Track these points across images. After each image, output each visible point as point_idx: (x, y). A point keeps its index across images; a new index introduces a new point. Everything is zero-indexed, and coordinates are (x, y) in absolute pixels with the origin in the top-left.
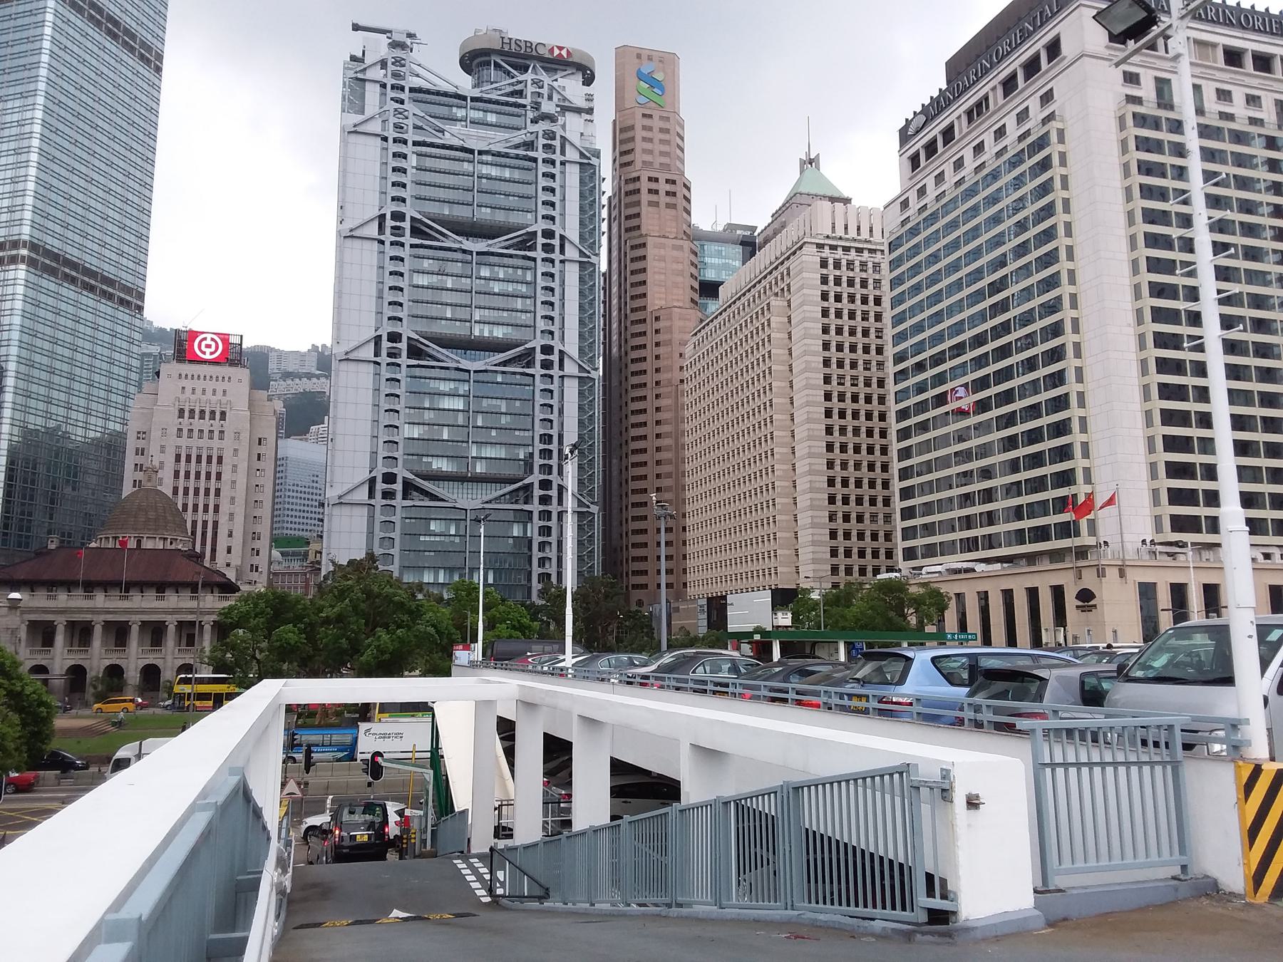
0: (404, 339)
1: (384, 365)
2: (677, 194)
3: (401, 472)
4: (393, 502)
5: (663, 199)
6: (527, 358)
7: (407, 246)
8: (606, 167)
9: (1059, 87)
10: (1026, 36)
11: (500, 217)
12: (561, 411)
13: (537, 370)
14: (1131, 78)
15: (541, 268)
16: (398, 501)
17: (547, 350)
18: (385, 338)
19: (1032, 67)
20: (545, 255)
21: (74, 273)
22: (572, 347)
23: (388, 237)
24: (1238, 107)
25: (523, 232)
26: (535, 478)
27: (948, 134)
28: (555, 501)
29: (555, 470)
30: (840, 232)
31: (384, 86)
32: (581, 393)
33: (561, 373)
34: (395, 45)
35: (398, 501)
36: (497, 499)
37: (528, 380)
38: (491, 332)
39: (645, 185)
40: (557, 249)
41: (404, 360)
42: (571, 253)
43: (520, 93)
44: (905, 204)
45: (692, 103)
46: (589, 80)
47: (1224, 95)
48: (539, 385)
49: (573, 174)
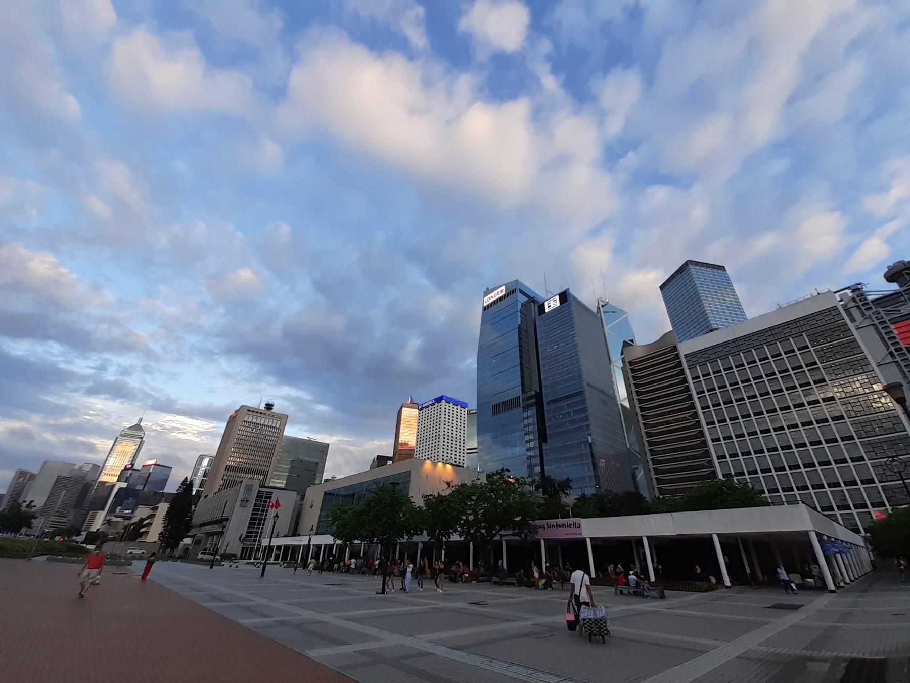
31: (858, 306)
34: (853, 291)
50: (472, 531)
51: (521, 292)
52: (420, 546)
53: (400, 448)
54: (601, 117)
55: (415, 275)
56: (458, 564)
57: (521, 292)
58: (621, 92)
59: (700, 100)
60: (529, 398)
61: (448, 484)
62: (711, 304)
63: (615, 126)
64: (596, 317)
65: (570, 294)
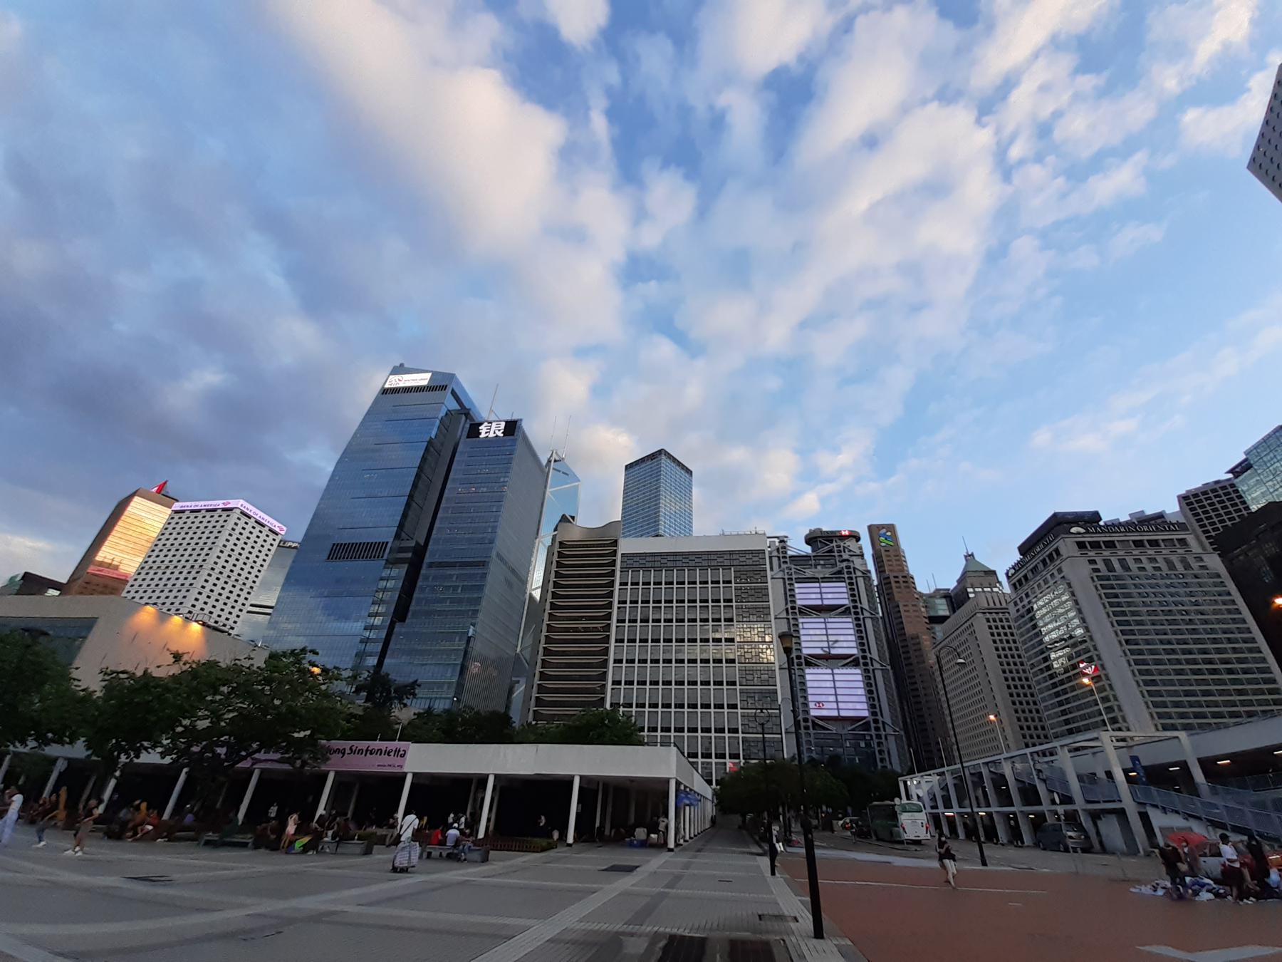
2: (908, 581)
5: (903, 585)
8: (874, 576)
9: (1065, 566)
10: (1045, 546)
14: (1092, 562)
19: (1050, 556)
22: (875, 655)
24: (1148, 566)
27: (1025, 577)
30: (992, 605)
39: (892, 580)
42: (867, 614)
43: (831, 551)
44: (1016, 604)
45: (907, 543)
46: (858, 539)
47: (1138, 560)
49: (861, 581)
50: (195, 749)
51: (453, 393)
52: (61, 766)
53: (92, 569)
54: (640, 215)
55: (261, 260)
56: (138, 808)
57: (453, 393)
58: (671, 197)
59: (738, 269)
60: (402, 550)
61: (177, 657)
62: (667, 505)
63: (650, 238)
64: (541, 472)
65: (520, 427)
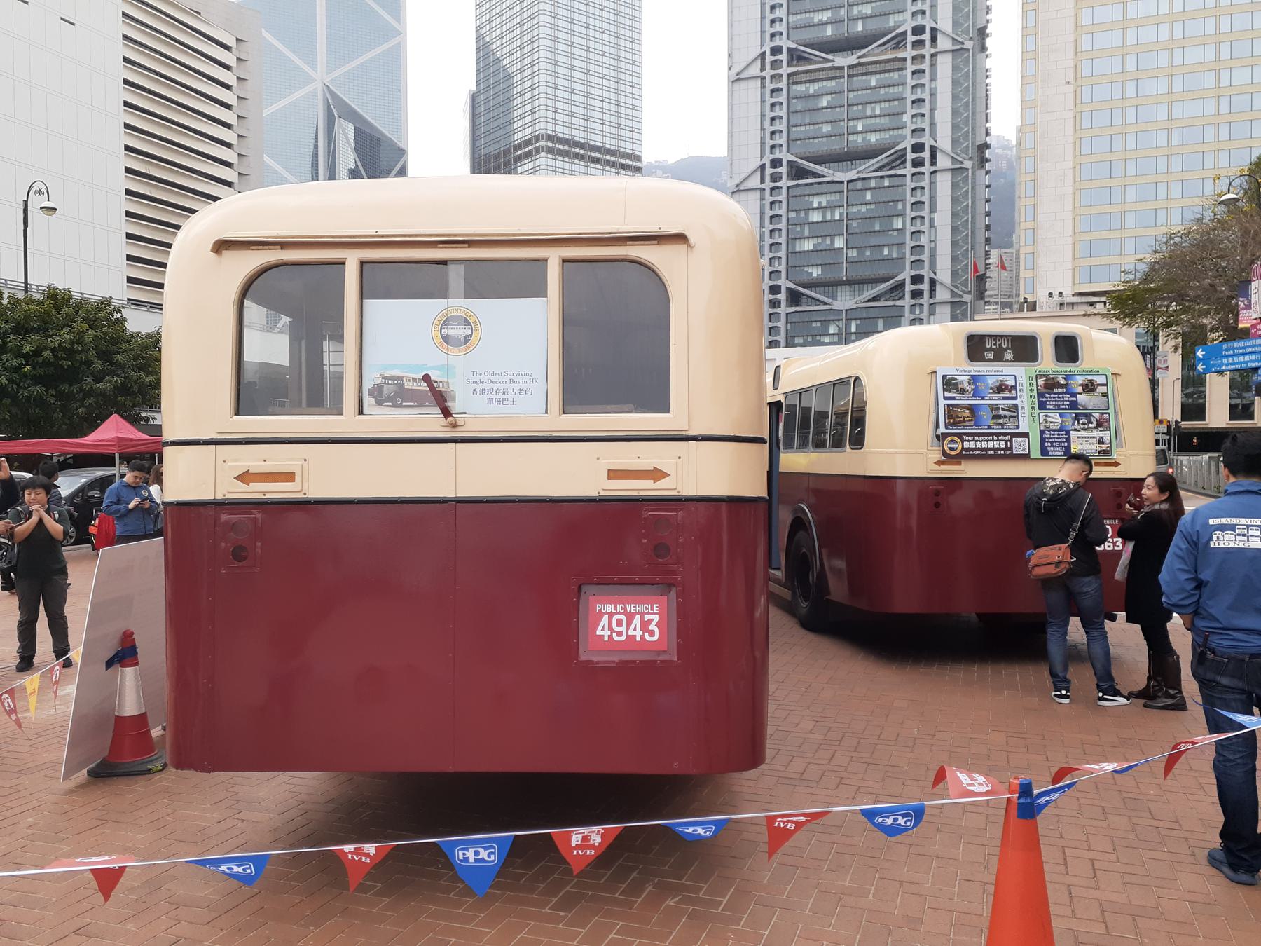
0: (784, 163)
1: (767, 192)
3: (784, 283)
4: (778, 310)
6: (900, 158)
7: (785, 78)
11: (874, 25)
12: (933, 209)
13: (908, 170)
15: (910, 67)
16: (783, 309)
17: (918, 148)
18: (768, 165)
20: (914, 53)
21: (582, 152)
22: (944, 143)
23: (768, 72)
25: (893, 34)
26: (906, 275)
28: (926, 294)
29: (926, 264)
32: (955, 186)
33: (933, 169)
35: (783, 309)
36: (874, 299)
37: (897, 181)
38: (864, 139)
40: (928, 43)
41: (785, 183)
42: (944, 43)
48: (909, 184)
